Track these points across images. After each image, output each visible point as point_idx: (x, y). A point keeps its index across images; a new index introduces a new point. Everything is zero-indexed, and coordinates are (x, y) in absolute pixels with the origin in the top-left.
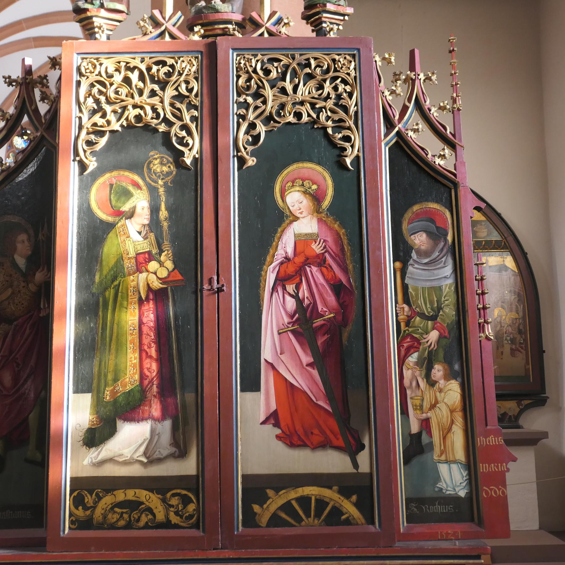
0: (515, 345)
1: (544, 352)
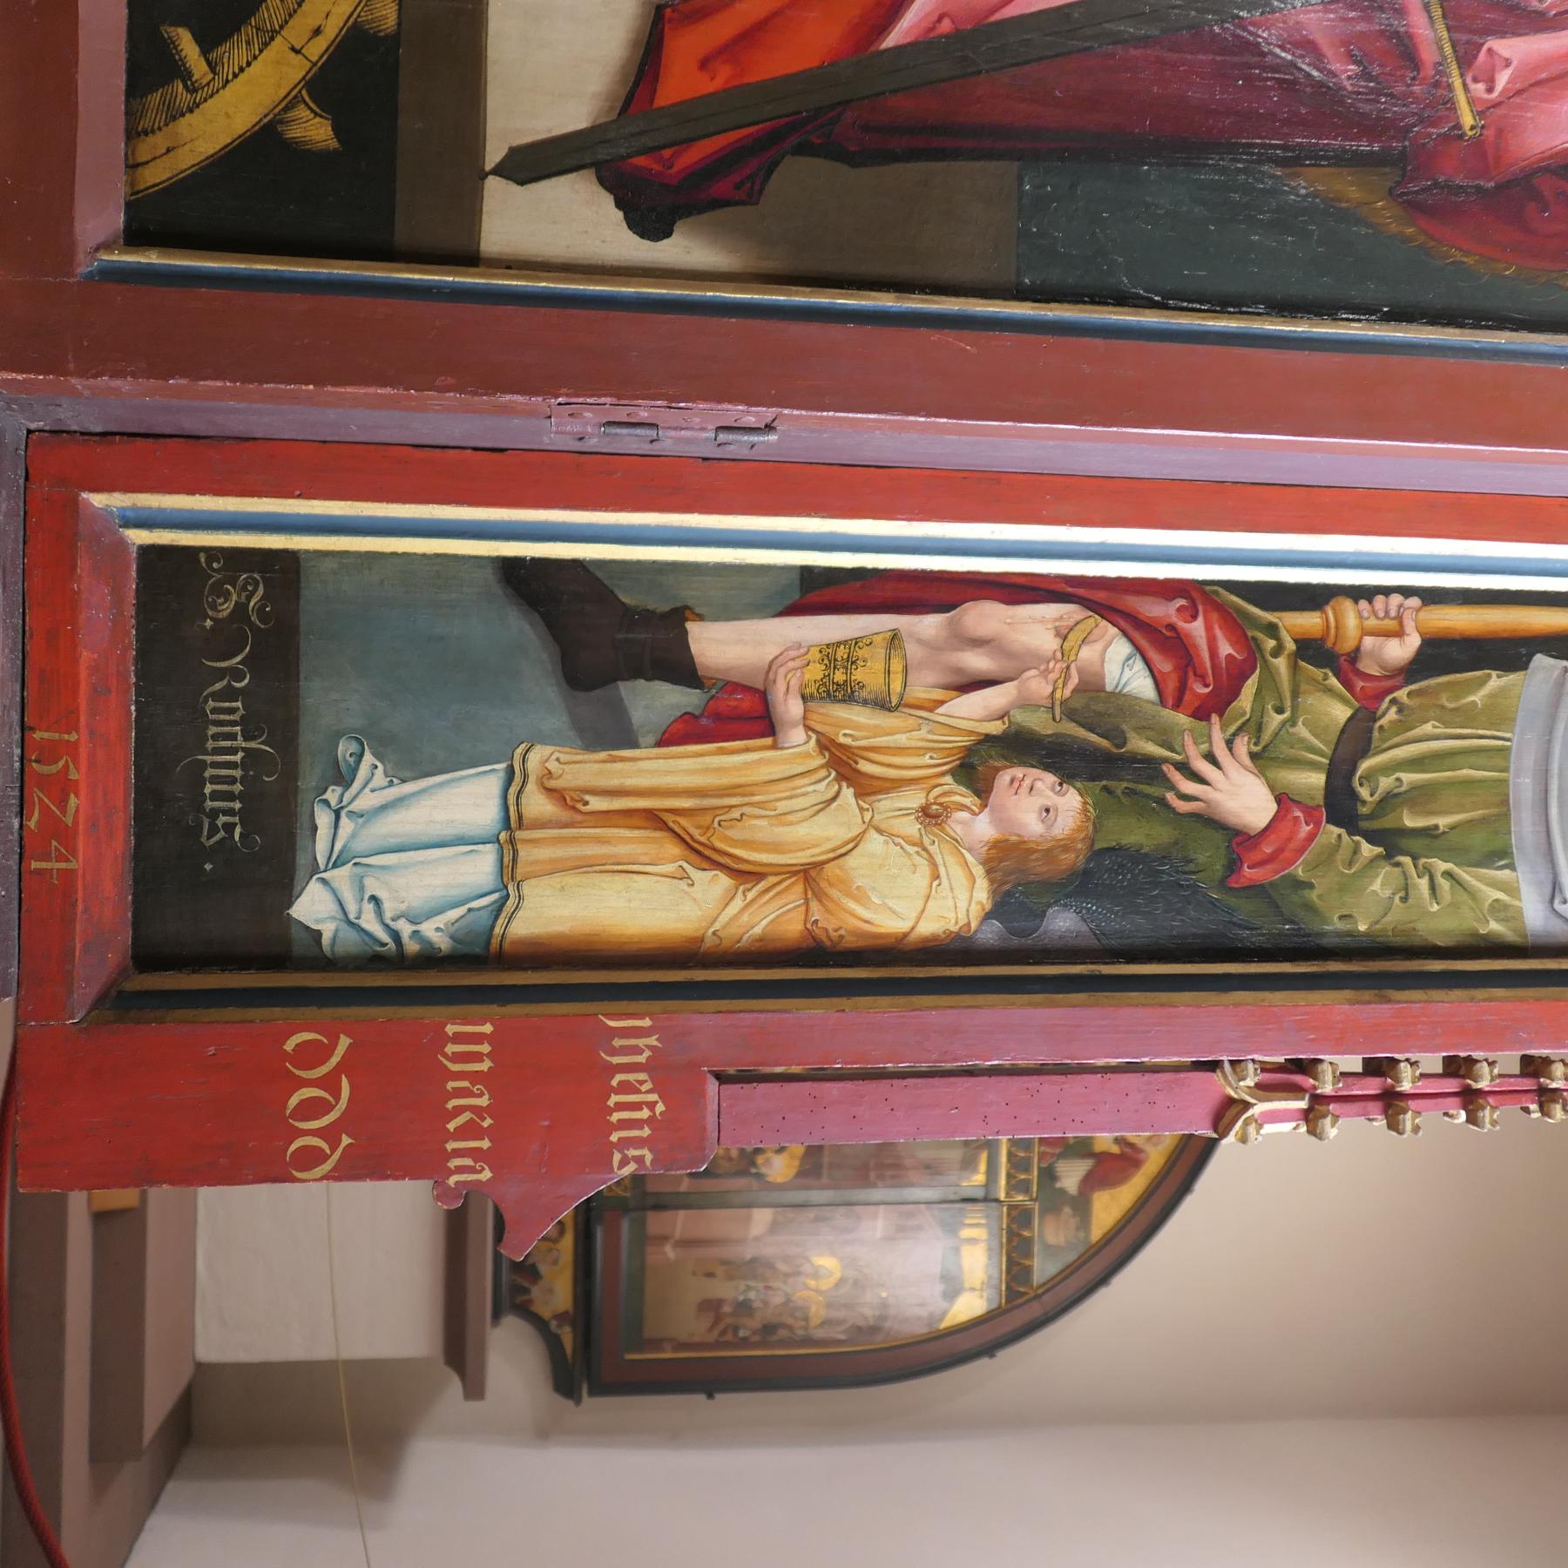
1: (710, 1396)
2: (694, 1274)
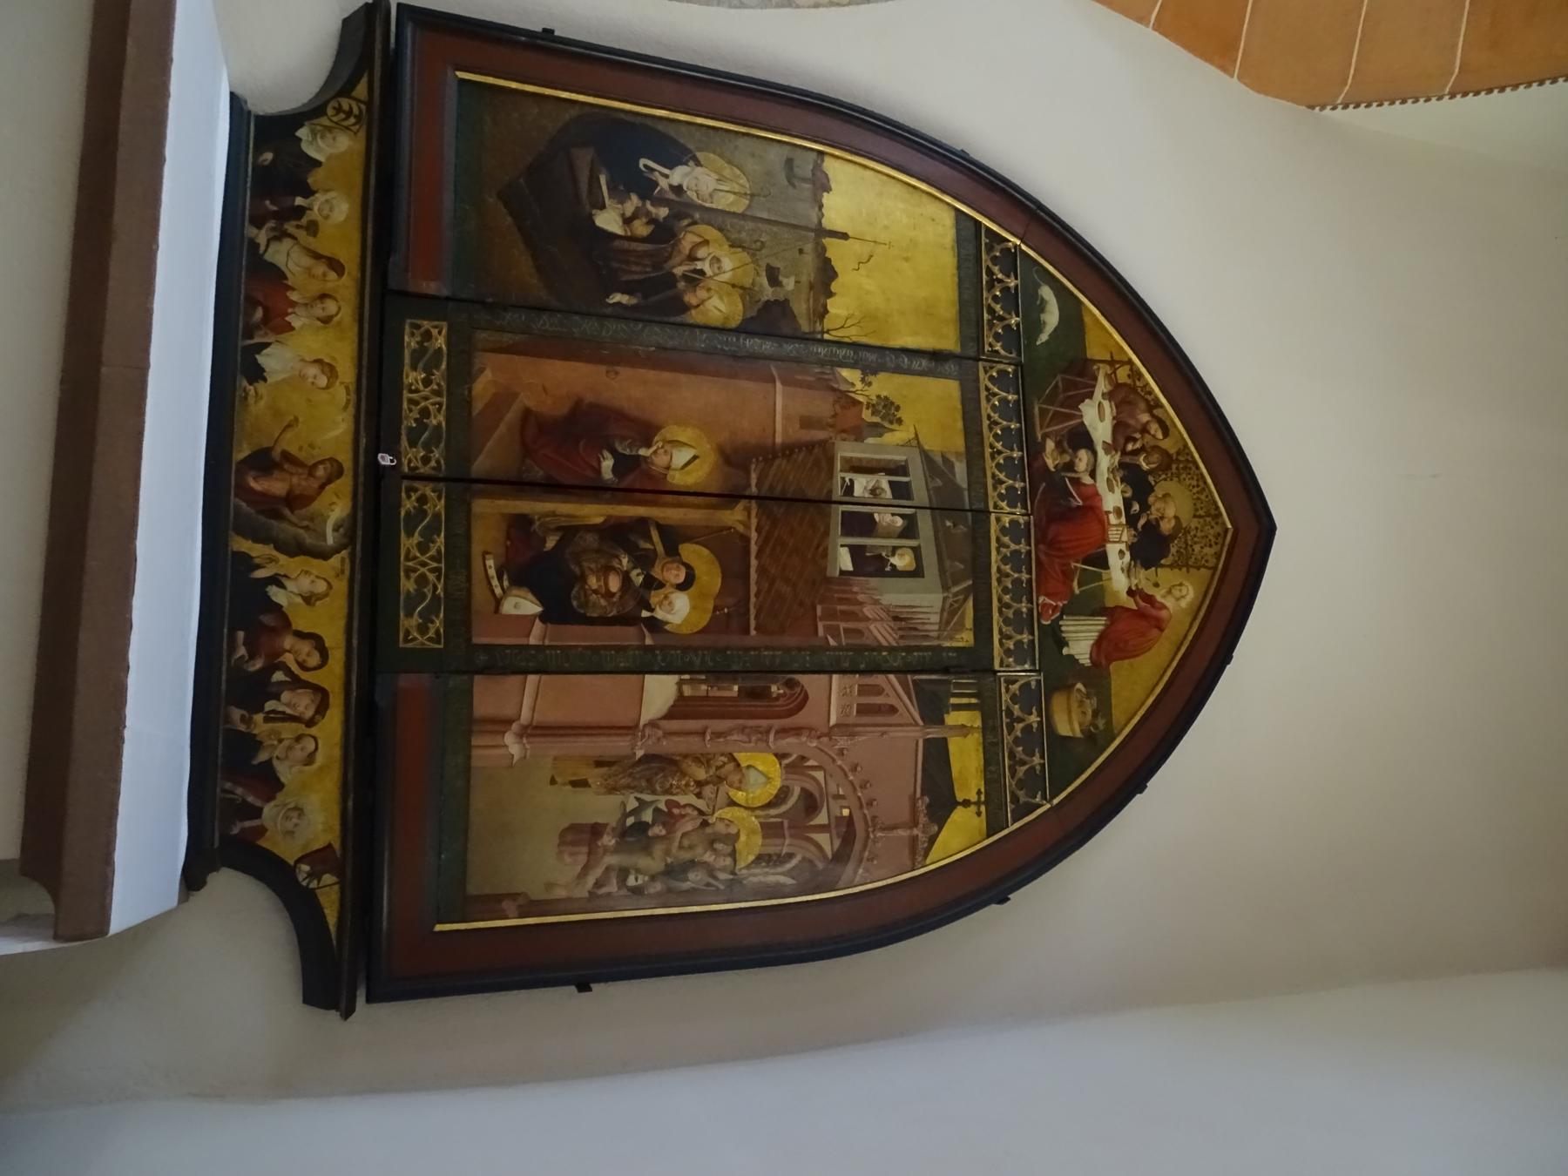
2: (553, 781)
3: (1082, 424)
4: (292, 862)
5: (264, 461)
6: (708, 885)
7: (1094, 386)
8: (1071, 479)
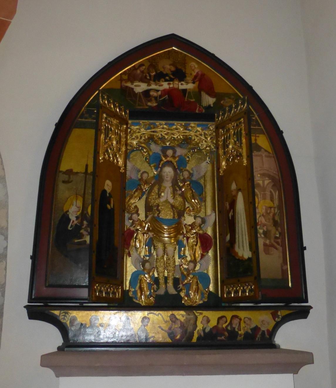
0: (270, 239)
3: (142, 92)
4: (276, 322)
5: (171, 334)
6: (278, 215)
7: (129, 87)
8: (159, 99)
